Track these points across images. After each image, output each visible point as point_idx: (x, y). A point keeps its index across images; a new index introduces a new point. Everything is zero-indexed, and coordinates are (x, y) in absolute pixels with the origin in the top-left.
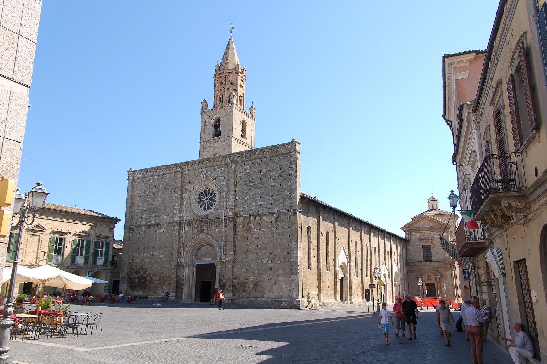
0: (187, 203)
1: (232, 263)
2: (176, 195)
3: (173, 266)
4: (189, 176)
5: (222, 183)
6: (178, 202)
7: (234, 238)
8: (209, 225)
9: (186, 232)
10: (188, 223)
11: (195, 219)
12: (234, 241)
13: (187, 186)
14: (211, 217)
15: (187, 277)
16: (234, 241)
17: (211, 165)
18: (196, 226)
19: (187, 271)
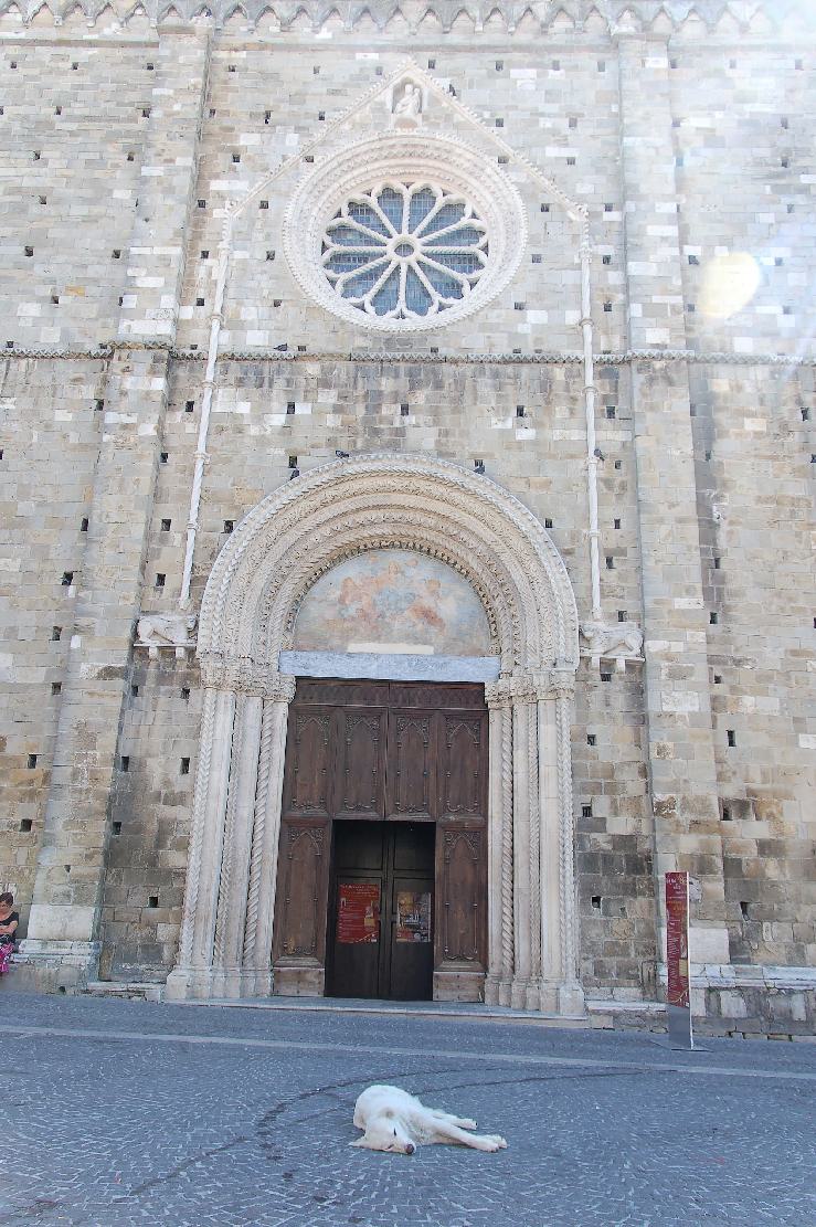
0: (241, 237)
1: (701, 673)
2: (153, 170)
3: (86, 669)
4: (266, 76)
5: (552, 152)
6: (170, 212)
7: (703, 506)
8: (457, 401)
9: (226, 427)
10: (249, 369)
11: (318, 342)
12: (709, 528)
13: (247, 140)
14: (478, 345)
15: (219, 778)
16: (709, 528)
17: (455, 38)
18: (329, 397)
19: (225, 719)
